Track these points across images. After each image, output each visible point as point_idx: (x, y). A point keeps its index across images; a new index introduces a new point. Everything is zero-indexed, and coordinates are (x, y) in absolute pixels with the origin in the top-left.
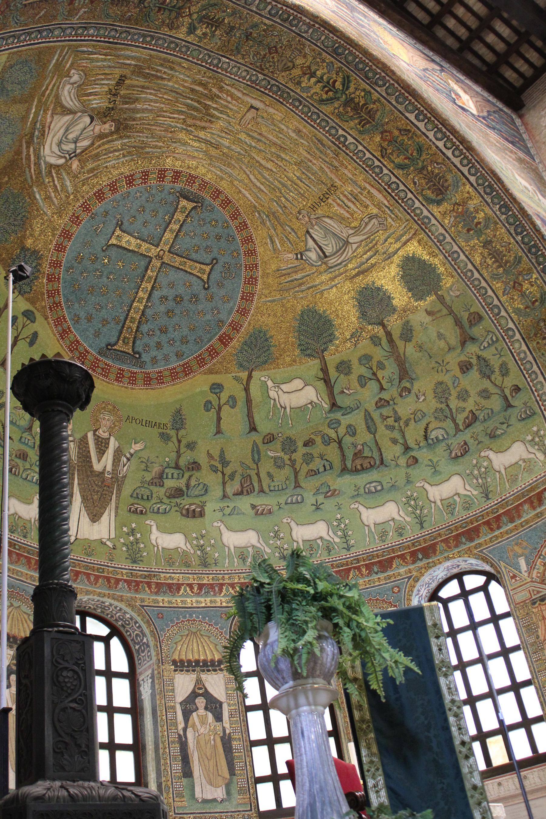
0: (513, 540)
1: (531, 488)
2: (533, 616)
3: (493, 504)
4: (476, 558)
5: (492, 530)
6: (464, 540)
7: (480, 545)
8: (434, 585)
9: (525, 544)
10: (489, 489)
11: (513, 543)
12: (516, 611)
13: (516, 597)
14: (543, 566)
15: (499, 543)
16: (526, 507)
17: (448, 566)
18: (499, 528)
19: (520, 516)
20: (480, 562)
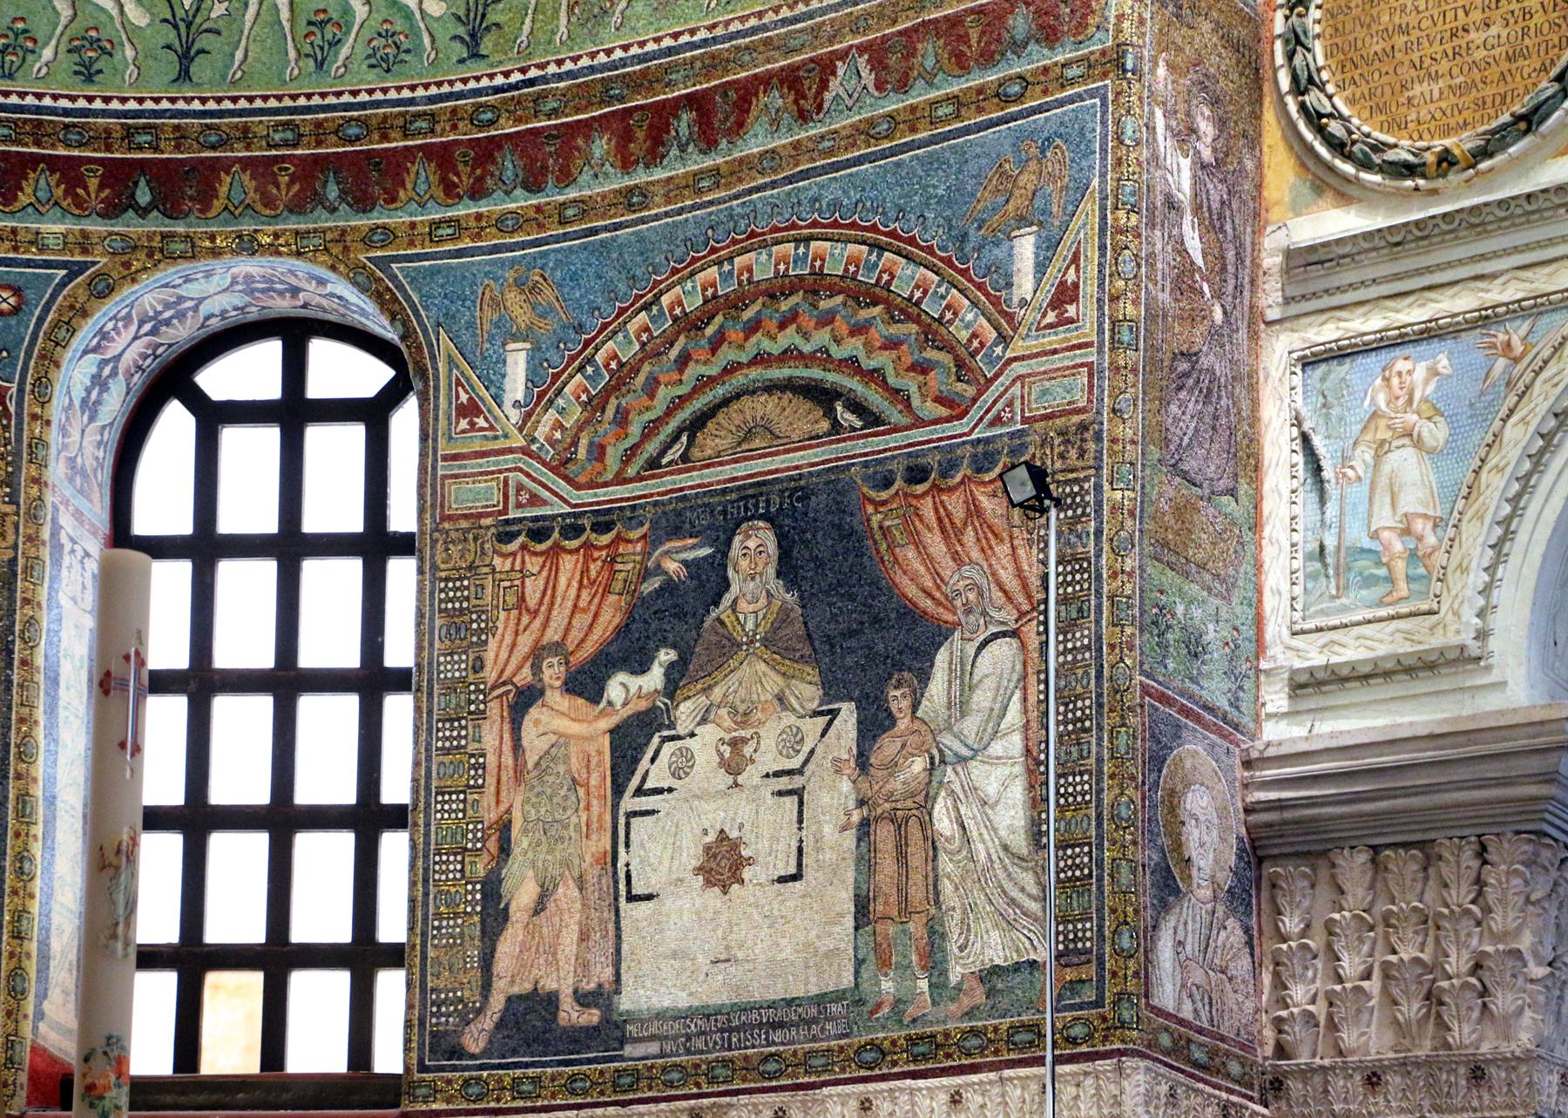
0: (513, 261)
1: (644, 73)
2: (489, 582)
3: (485, 82)
4: (355, 284)
5: (451, 192)
6: (333, 192)
7: (388, 235)
8: (183, 333)
9: (549, 294)
10: (492, 17)
11: (510, 275)
12: (434, 542)
13: (452, 488)
14: (584, 405)
15: (460, 253)
16: (601, 146)
17: (249, 278)
18: (477, 193)
19: (566, 178)
20: (370, 307)
